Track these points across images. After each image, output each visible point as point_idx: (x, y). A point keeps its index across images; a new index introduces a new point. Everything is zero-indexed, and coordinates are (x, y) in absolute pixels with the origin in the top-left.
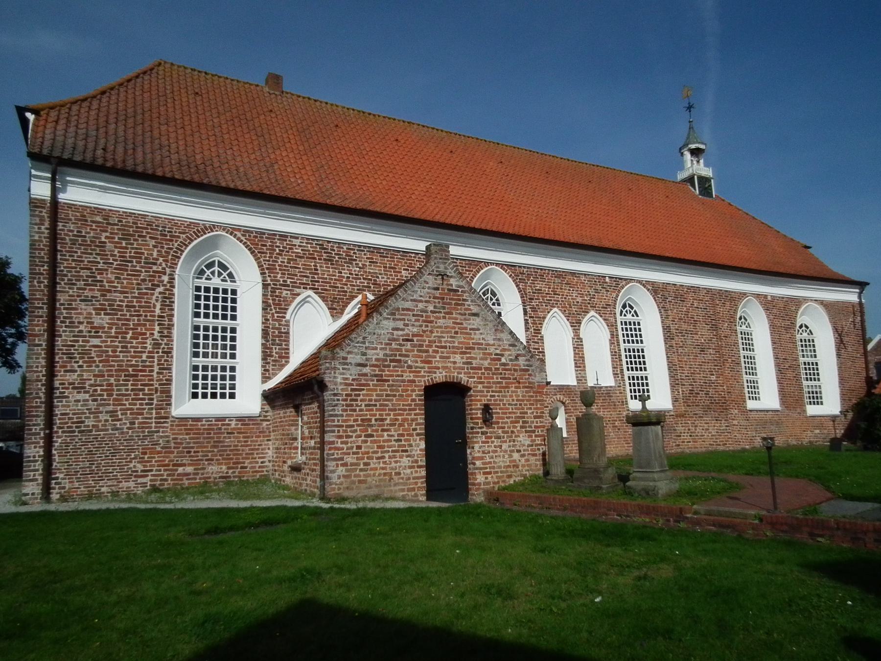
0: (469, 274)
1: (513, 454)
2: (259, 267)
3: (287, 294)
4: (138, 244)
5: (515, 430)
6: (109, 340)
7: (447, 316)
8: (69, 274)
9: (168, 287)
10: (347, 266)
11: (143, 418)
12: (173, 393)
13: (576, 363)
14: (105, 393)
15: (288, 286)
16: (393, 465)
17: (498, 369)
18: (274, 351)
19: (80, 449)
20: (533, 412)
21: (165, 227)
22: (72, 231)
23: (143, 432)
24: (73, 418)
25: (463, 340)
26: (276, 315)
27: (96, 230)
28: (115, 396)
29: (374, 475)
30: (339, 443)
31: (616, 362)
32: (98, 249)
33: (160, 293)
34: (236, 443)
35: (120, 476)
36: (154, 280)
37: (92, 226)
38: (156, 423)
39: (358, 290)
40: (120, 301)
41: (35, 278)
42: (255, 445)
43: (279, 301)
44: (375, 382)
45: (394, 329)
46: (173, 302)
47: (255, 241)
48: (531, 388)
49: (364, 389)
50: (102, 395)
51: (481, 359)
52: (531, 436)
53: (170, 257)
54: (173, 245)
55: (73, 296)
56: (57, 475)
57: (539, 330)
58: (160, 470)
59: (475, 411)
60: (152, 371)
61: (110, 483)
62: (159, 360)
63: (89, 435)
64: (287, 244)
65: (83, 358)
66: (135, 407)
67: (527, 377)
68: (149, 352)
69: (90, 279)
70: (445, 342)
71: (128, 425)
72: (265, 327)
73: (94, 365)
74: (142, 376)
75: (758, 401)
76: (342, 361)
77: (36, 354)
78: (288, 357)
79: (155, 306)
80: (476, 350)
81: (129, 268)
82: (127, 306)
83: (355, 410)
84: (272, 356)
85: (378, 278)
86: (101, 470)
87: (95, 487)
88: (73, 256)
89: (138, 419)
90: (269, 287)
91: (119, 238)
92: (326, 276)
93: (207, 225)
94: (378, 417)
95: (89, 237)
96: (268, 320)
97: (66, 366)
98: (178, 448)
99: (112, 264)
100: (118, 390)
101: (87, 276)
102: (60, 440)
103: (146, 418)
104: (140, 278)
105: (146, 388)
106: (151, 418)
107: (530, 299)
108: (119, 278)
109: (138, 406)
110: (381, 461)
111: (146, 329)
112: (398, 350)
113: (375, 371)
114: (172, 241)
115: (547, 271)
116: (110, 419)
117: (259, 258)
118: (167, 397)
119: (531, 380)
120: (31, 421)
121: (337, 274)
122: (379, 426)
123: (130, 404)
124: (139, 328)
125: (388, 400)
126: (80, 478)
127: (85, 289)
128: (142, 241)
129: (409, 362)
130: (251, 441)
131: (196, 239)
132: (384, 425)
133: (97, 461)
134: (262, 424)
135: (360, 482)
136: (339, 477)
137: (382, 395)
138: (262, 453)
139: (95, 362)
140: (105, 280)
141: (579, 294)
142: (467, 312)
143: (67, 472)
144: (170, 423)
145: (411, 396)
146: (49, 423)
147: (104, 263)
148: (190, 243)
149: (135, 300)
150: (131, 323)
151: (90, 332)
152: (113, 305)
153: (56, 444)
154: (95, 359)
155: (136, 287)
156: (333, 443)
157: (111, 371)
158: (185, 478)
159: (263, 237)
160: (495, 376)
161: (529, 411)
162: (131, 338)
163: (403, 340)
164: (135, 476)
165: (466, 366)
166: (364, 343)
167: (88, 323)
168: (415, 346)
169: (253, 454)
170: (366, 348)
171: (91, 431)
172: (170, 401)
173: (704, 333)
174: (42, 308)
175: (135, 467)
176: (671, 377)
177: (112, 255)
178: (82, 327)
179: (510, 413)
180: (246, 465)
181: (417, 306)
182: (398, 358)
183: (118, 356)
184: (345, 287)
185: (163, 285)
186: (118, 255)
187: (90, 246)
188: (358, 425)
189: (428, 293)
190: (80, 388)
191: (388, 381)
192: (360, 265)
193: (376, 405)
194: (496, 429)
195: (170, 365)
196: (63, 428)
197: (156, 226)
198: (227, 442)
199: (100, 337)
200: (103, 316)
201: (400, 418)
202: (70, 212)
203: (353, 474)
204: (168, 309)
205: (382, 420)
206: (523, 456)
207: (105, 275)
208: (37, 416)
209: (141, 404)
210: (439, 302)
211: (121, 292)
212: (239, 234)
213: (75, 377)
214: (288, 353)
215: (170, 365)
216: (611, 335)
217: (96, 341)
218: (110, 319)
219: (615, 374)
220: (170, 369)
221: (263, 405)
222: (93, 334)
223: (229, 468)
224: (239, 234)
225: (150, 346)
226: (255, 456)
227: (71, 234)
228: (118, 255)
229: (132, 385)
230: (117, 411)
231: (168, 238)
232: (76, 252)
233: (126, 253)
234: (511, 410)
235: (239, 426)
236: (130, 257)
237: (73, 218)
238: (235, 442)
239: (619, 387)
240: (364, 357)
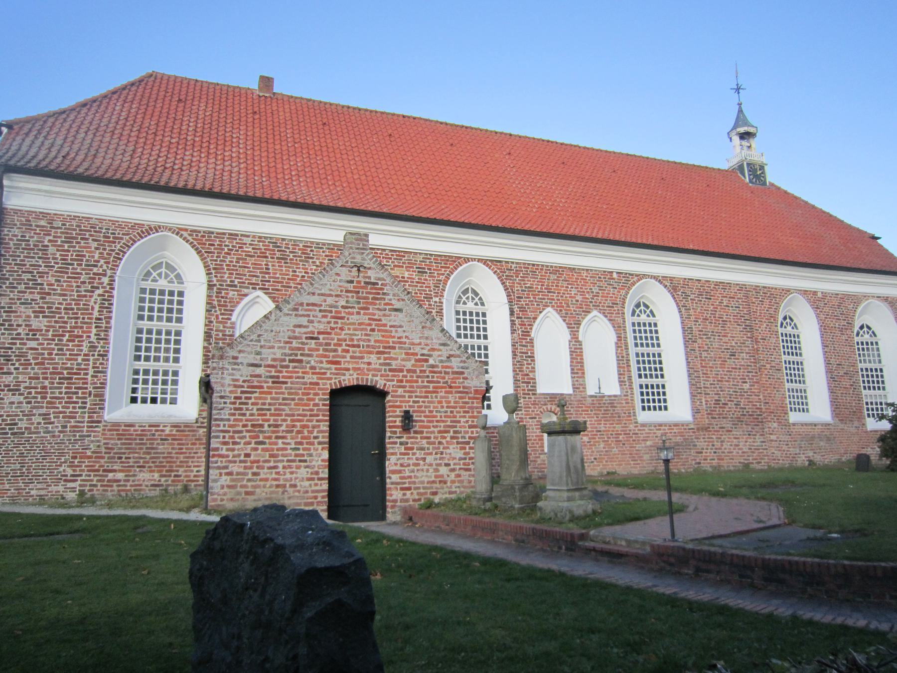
0: (445, 271)
1: (440, 468)
2: (205, 267)
3: (234, 295)
4: (80, 247)
5: (444, 441)
6: (46, 342)
7: (362, 312)
8: (11, 278)
9: (108, 289)
10: (303, 265)
12: (107, 397)
13: (572, 369)
15: (236, 286)
16: (288, 476)
17: (424, 371)
20: (467, 422)
21: (109, 229)
23: (75, 436)
24: (6, 420)
25: (381, 338)
26: (221, 317)
27: (40, 234)
28: (48, 399)
29: (264, 486)
30: (224, 450)
31: (624, 367)
32: (40, 252)
33: (99, 295)
34: (170, 451)
35: (50, 479)
37: (36, 230)
38: (88, 427)
40: (59, 303)
42: (190, 453)
43: (225, 302)
44: (270, 384)
45: (295, 326)
46: (112, 304)
47: (202, 240)
48: (467, 393)
49: (256, 392)
50: (36, 398)
51: (403, 360)
52: (465, 448)
53: (112, 259)
54: (115, 247)
55: (13, 299)
57: (528, 332)
58: (90, 476)
59: (393, 418)
61: (39, 486)
62: (94, 363)
64: (237, 243)
65: (20, 360)
66: (68, 410)
67: (462, 380)
68: (85, 355)
69: (31, 283)
70: (358, 340)
71: (60, 429)
73: (30, 367)
74: (76, 379)
75: (806, 413)
76: (232, 361)
79: (93, 308)
80: (397, 350)
82: (65, 309)
83: (244, 415)
86: (32, 473)
88: (16, 260)
89: (70, 422)
92: (278, 275)
94: (272, 422)
95: (33, 241)
96: (211, 322)
98: (110, 453)
99: (53, 267)
100: (52, 393)
101: (28, 280)
103: (79, 422)
105: (80, 391)
106: (83, 422)
107: (518, 297)
108: (59, 281)
109: (71, 410)
110: (274, 471)
112: (299, 349)
113: (270, 372)
114: (114, 242)
115: (540, 267)
116: (43, 422)
117: (205, 258)
118: (100, 400)
119: (466, 384)
121: (291, 273)
122: (273, 432)
123: (63, 407)
124: (76, 330)
125: (285, 404)
126: (10, 480)
127: (25, 292)
128: (85, 243)
129: (313, 363)
130: (187, 449)
131: (139, 240)
132: (278, 432)
133: (28, 463)
134: (198, 431)
135: (247, 493)
136: (222, 487)
137: (278, 399)
138: (198, 462)
139: (31, 364)
140: (45, 284)
141: (578, 291)
142: (388, 307)
144: (102, 428)
145: (313, 400)
147: (45, 266)
148: (132, 244)
149: (73, 302)
150: (68, 326)
152: (51, 308)
154: (32, 361)
155: (75, 289)
156: (217, 449)
157: (46, 373)
158: (115, 484)
159: (211, 237)
160: (420, 380)
161: (462, 420)
162: (68, 341)
163: (306, 338)
164: (65, 481)
165: (383, 368)
166: (259, 341)
167: (26, 325)
168: (321, 345)
169: (187, 462)
170: (261, 347)
171: (23, 433)
172: (103, 404)
173: (736, 334)
176: (691, 385)
177: (54, 258)
178: (20, 330)
179: (437, 421)
180: (180, 473)
181: (325, 301)
182: (299, 357)
183: (54, 359)
185: (102, 287)
186: (60, 258)
187: (33, 249)
188: (248, 431)
189: (340, 286)
190: (15, 390)
191: (286, 383)
192: (318, 263)
193: (269, 410)
194: (419, 440)
195: (105, 368)
197: (99, 228)
198: (160, 449)
199: (38, 339)
201: (298, 424)
202: (16, 218)
203: (239, 484)
204: (107, 312)
205: (277, 426)
206: (453, 470)
207: (45, 278)
209: (74, 408)
210: (353, 297)
211: (61, 295)
212: (185, 234)
213: (11, 379)
215: (105, 368)
216: (618, 337)
217: (33, 344)
218: (48, 322)
219: (621, 382)
221: (201, 411)
222: (30, 336)
224: (185, 234)
226: (190, 464)
227: (15, 238)
228: (60, 258)
229: (66, 388)
230: (49, 414)
231: (111, 239)
232: (19, 256)
233: (67, 255)
234: (439, 418)
235: (174, 433)
236: (72, 260)
237: (18, 223)
238: (168, 448)
239: (625, 396)
240: (259, 357)
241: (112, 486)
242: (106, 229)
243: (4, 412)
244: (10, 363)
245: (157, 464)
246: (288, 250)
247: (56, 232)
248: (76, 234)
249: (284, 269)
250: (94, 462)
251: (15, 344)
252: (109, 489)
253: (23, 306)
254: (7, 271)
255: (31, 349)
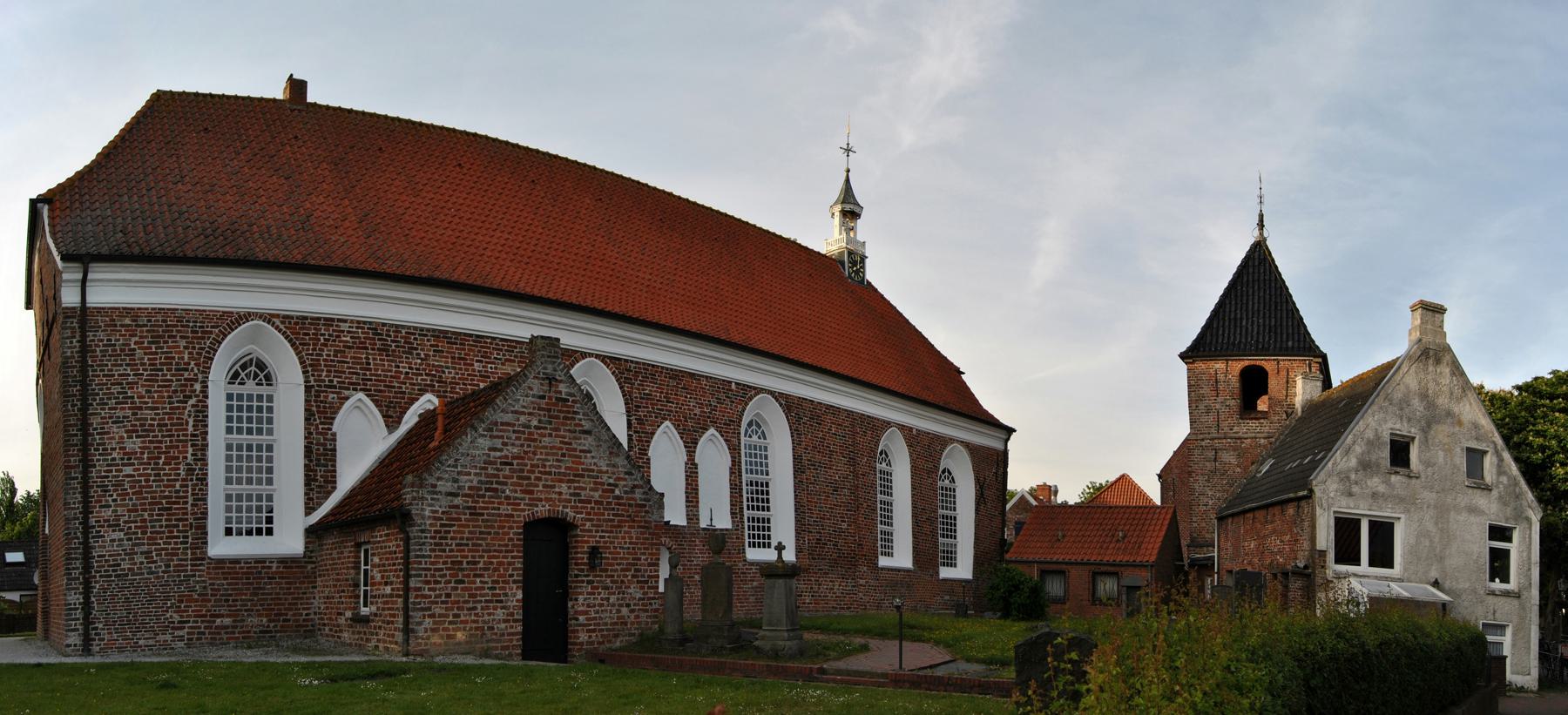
3: (333, 398)
6: (142, 467)
9: (201, 398)
11: (178, 560)
14: (139, 531)
15: (335, 387)
18: (319, 474)
19: (118, 595)
22: (102, 341)
23: (179, 576)
26: (320, 427)
27: (125, 335)
33: (193, 406)
36: (185, 391)
38: (192, 565)
39: (419, 390)
41: (68, 401)
42: (299, 594)
46: (207, 416)
54: (205, 343)
55: (105, 418)
56: (96, 625)
58: (197, 622)
60: (186, 503)
62: (193, 490)
63: (126, 580)
64: (334, 331)
68: (183, 480)
69: (121, 396)
71: (163, 569)
72: (308, 443)
73: (127, 498)
77: (74, 488)
78: (335, 482)
81: (160, 378)
84: (316, 481)
85: (444, 372)
87: (133, 639)
88: (104, 370)
89: (173, 560)
90: (313, 390)
91: (149, 342)
92: (379, 372)
93: (242, 313)
97: (101, 501)
98: (216, 595)
99: (143, 374)
100: (152, 527)
101: (118, 393)
102: (97, 586)
103: (181, 560)
104: (171, 390)
105: (181, 524)
106: (186, 560)
108: (150, 392)
111: (180, 452)
114: (203, 338)
116: (145, 561)
117: (301, 352)
118: (202, 534)
120: (71, 564)
124: (172, 451)
126: (117, 629)
128: (172, 342)
131: (229, 333)
133: (134, 609)
134: (306, 567)
138: (307, 604)
143: (106, 622)
146: (87, 568)
147: (134, 375)
148: (223, 339)
149: (167, 417)
150: (163, 445)
151: (123, 459)
153: (95, 590)
158: (223, 631)
159: (305, 323)
162: (164, 464)
164: (173, 628)
167: (120, 448)
169: (296, 604)
171: (127, 575)
172: (206, 538)
174: (76, 435)
175: (171, 617)
178: (115, 455)
180: (288, 617)
184: (404, 386)
185: (196, 396)
190: (115, 526)
192: (423, 356)
196: (100, 571)
197: (187, 321)
199: (133, 464)
200: (135, 439)
208: (76, 559)
209: (176, 543)
212: (277, 322)
213: (110, 513)
214: (335, 477)
217: (128, 470)
220: (205, 500)
221: (306, 543)
222: (125, 461)
223: (270, 621)
224: (277, 322)
225: (183, 473)
229: (166, 520)
230: (151, 552)
231: (200, 335)
232: (107, 365)
233: (156, 359)
236: (161, 364)
237: (102, 325)
241: (219, 633)
242: (193, 322)
243: (107, 552)
244: (108, 494)
245: (266, 607)
246: (389, 339)
247: (142, 332)
248: (163, 331)
249: (386, 363)
250: (200, 606)
251: (111, 471)
252: (218, 637)
253: (115, 426)
254: (96, 385)
255: (128, 476)
